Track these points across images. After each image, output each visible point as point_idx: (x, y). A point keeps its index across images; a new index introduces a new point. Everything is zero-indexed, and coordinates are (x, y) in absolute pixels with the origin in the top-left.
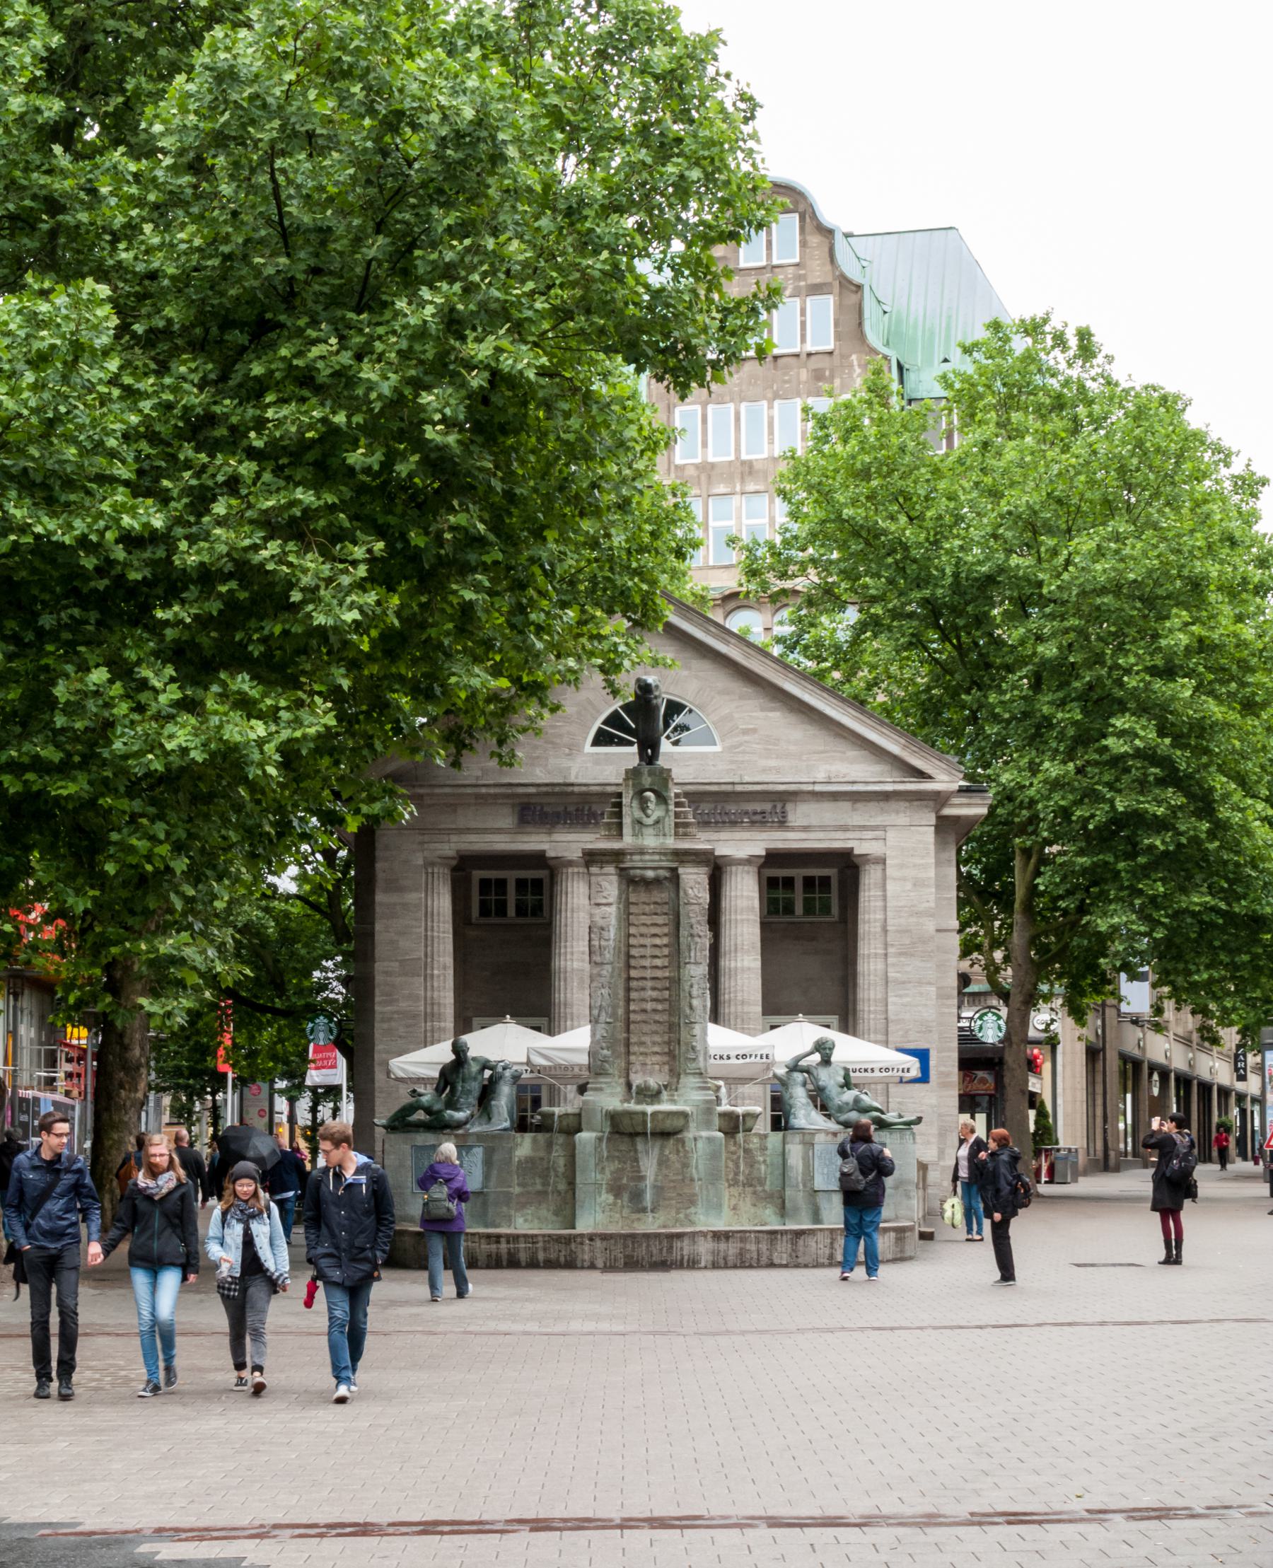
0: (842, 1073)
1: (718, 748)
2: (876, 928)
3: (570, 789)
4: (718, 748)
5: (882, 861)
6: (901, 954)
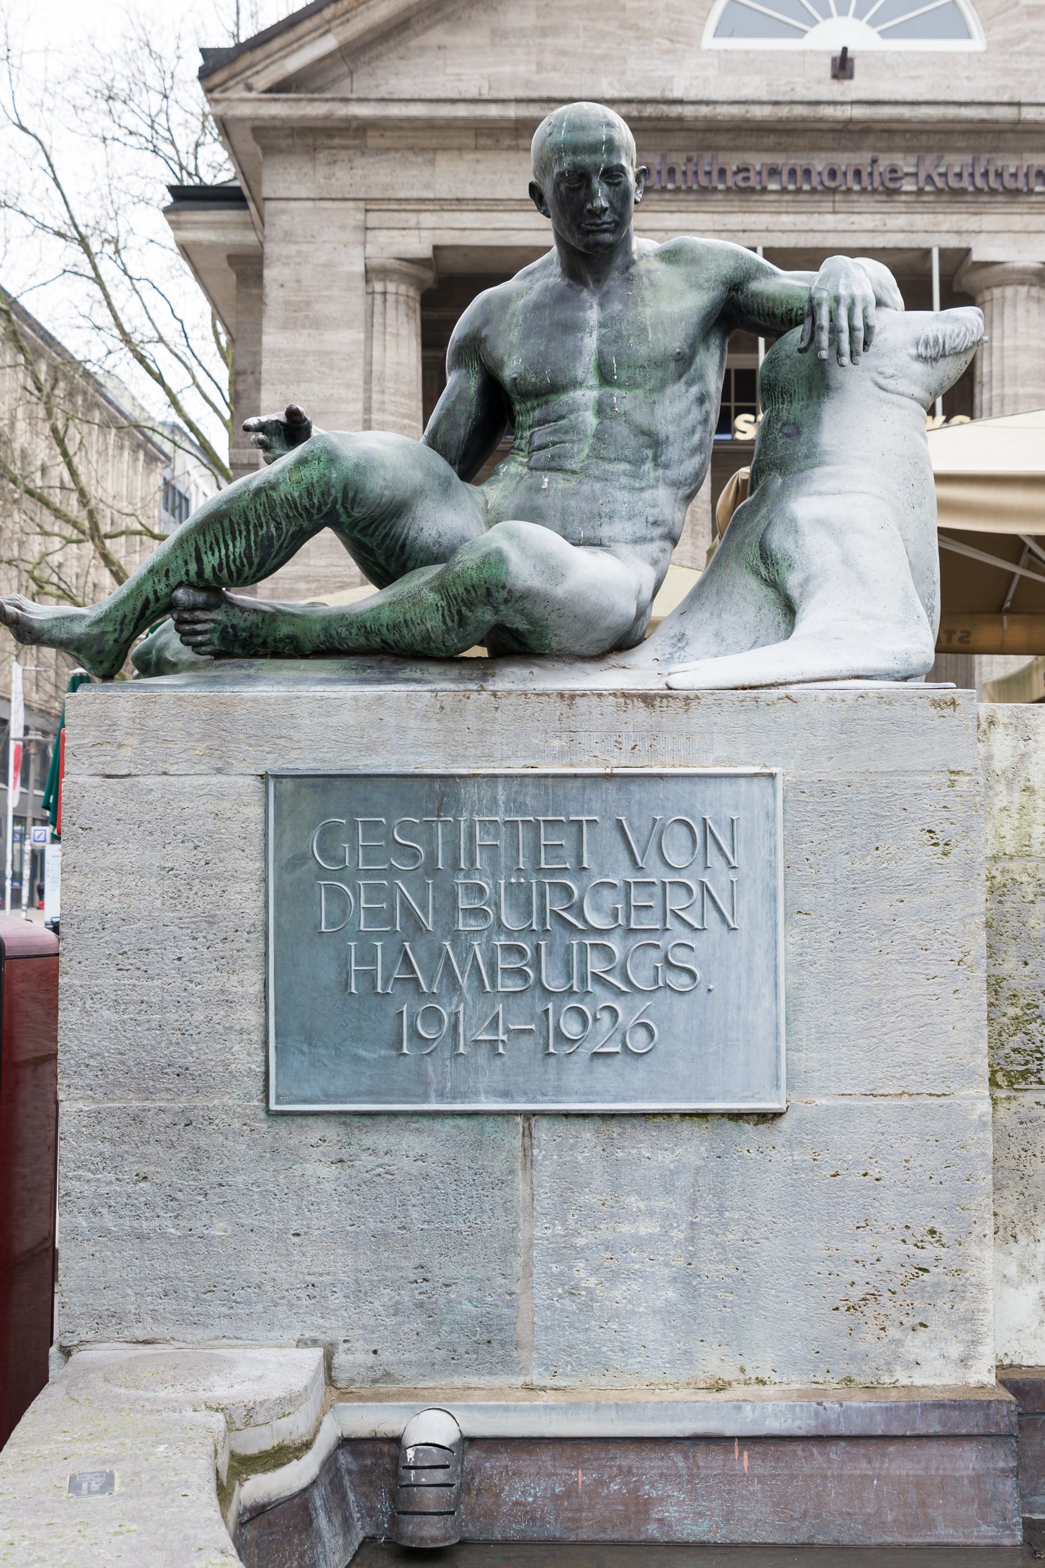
1: (977, 44)
3: (676, 111)
4: (977, 44)
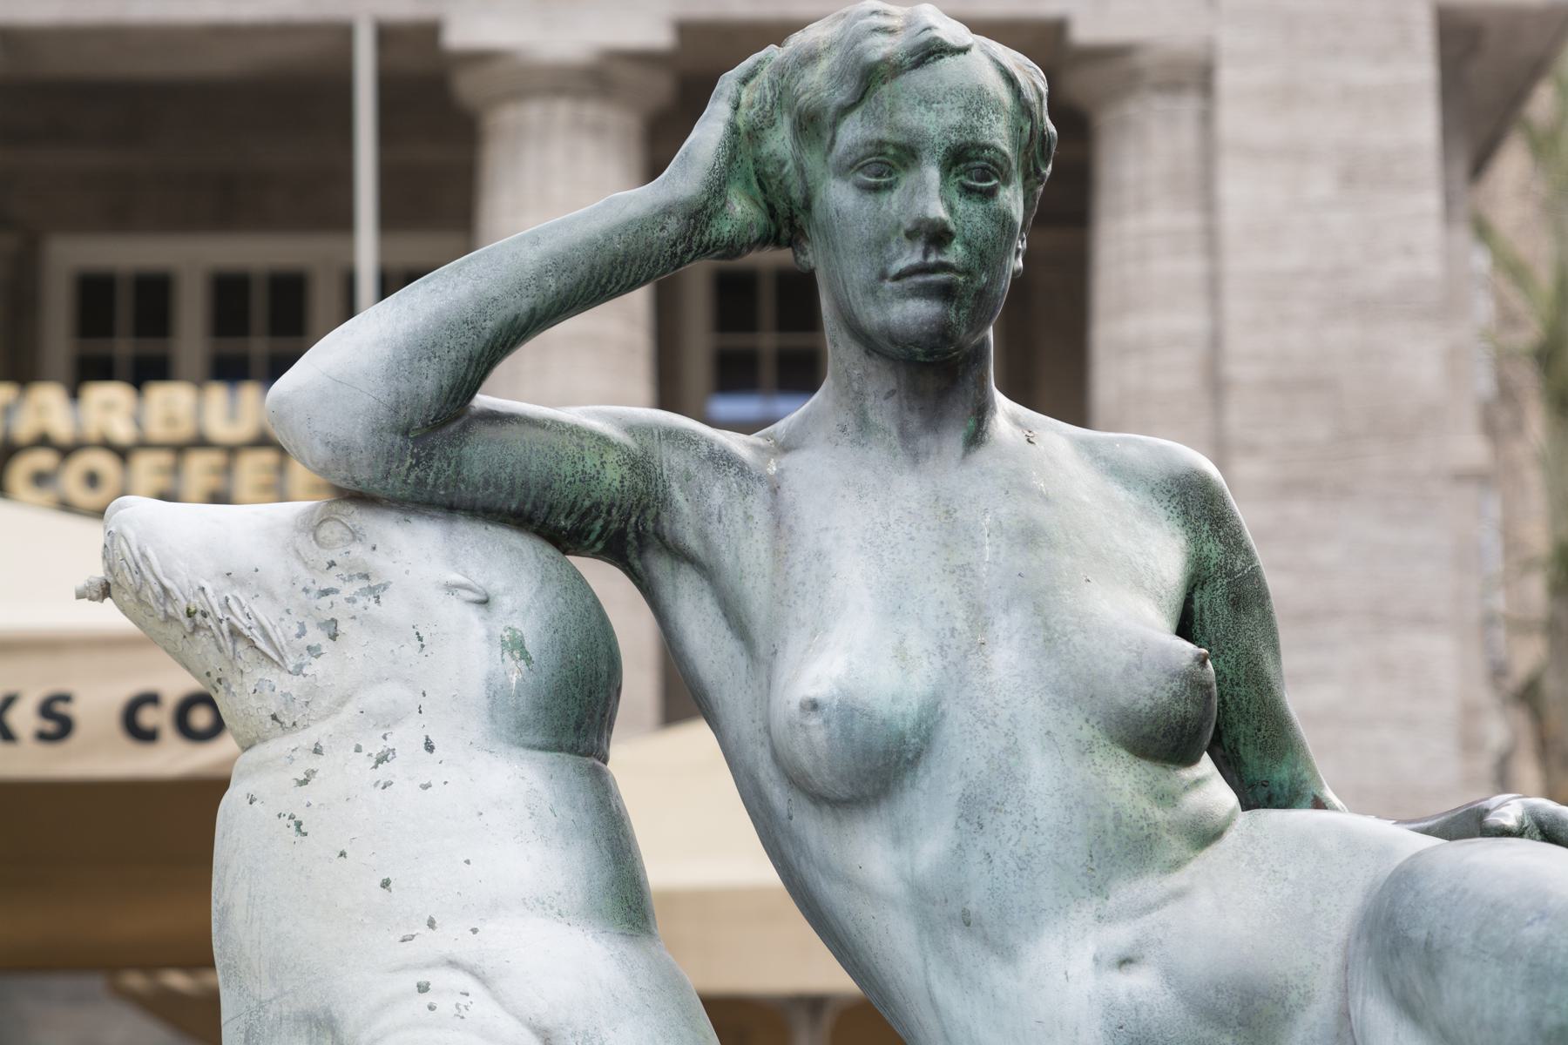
0: (1165, 555)
2: (1176, 374)
5: (1197, 77)
6: (1288, 488)
